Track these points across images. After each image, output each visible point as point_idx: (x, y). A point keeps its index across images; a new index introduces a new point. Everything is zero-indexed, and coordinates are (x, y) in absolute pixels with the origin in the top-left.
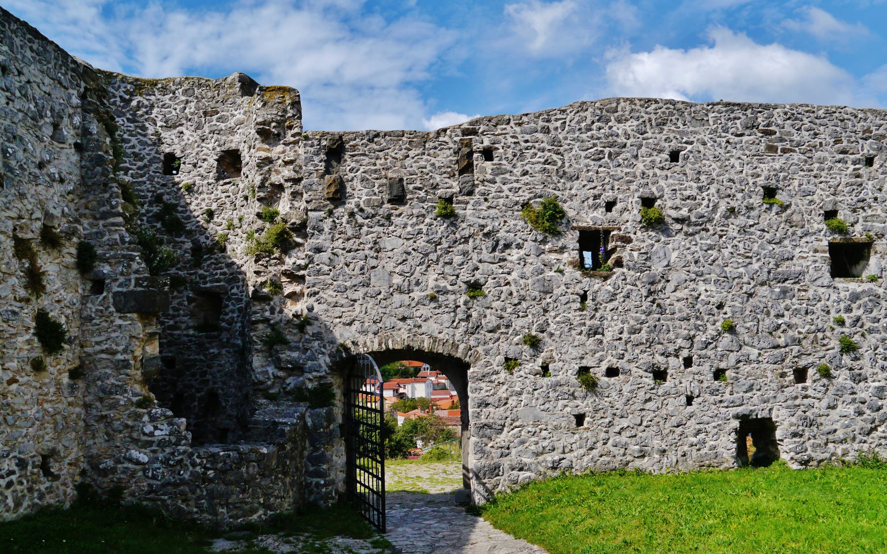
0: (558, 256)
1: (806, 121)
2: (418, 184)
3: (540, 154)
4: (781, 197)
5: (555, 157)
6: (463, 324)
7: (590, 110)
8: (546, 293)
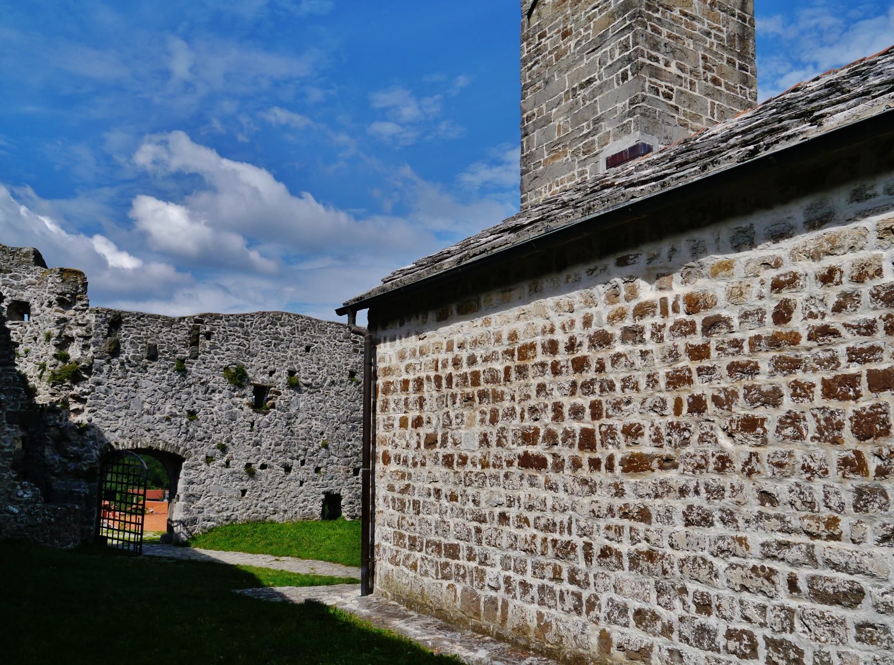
0: (241, 400)
2: (165, 349)
3: (237, 339)
5: (245, 342)
6: (184, 435)
7: (267, 317)
8: (232, 420)
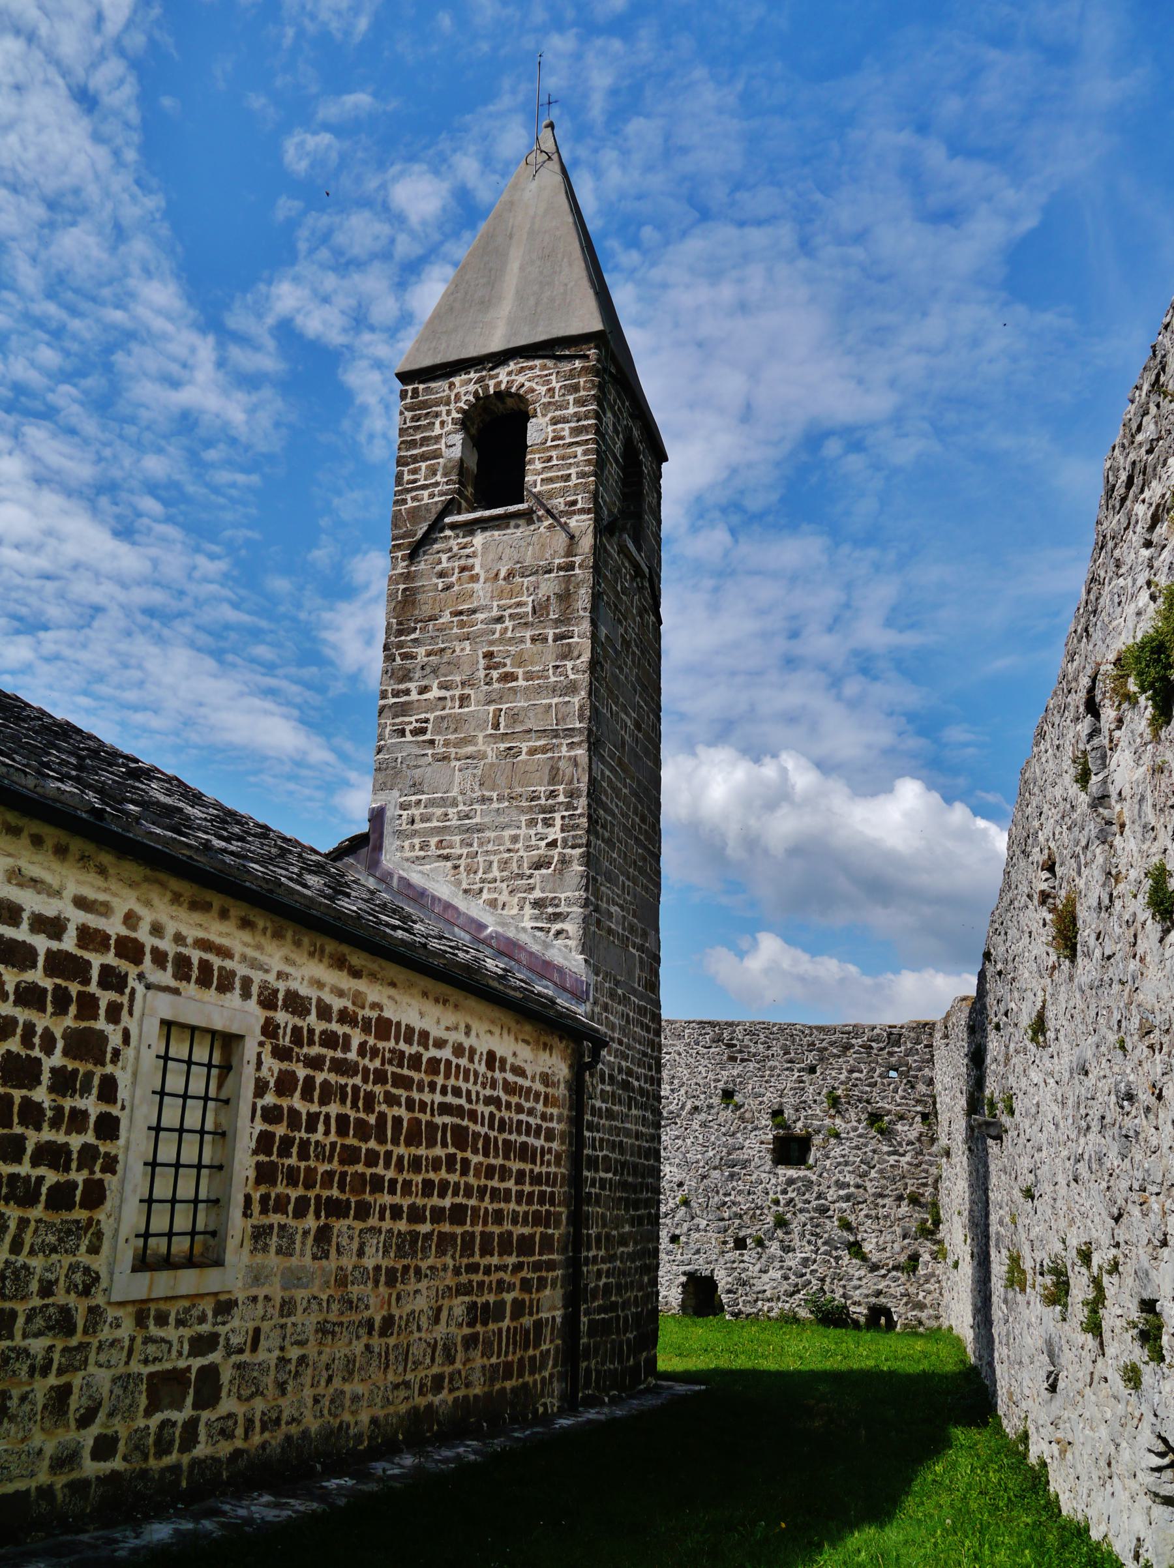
1: (762, 1036)
4: (738, 1098)
